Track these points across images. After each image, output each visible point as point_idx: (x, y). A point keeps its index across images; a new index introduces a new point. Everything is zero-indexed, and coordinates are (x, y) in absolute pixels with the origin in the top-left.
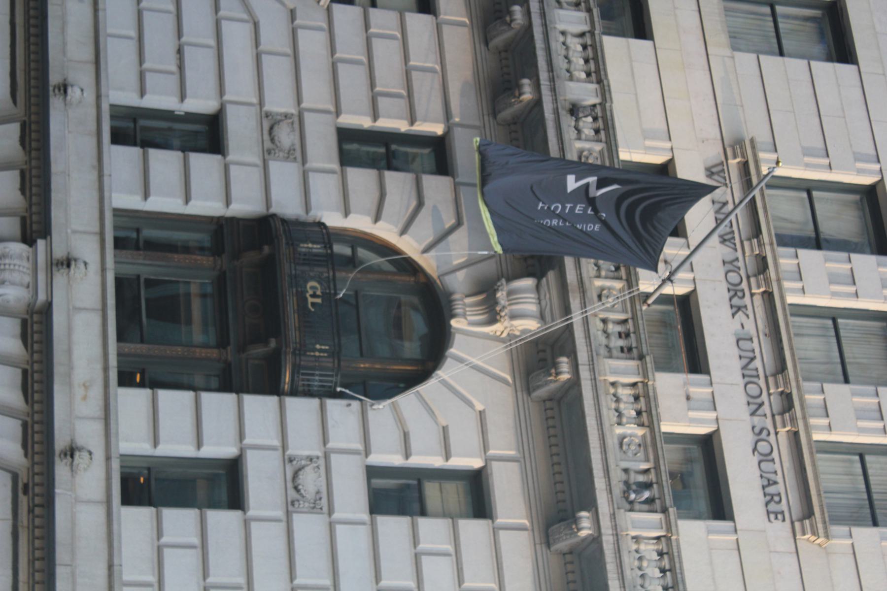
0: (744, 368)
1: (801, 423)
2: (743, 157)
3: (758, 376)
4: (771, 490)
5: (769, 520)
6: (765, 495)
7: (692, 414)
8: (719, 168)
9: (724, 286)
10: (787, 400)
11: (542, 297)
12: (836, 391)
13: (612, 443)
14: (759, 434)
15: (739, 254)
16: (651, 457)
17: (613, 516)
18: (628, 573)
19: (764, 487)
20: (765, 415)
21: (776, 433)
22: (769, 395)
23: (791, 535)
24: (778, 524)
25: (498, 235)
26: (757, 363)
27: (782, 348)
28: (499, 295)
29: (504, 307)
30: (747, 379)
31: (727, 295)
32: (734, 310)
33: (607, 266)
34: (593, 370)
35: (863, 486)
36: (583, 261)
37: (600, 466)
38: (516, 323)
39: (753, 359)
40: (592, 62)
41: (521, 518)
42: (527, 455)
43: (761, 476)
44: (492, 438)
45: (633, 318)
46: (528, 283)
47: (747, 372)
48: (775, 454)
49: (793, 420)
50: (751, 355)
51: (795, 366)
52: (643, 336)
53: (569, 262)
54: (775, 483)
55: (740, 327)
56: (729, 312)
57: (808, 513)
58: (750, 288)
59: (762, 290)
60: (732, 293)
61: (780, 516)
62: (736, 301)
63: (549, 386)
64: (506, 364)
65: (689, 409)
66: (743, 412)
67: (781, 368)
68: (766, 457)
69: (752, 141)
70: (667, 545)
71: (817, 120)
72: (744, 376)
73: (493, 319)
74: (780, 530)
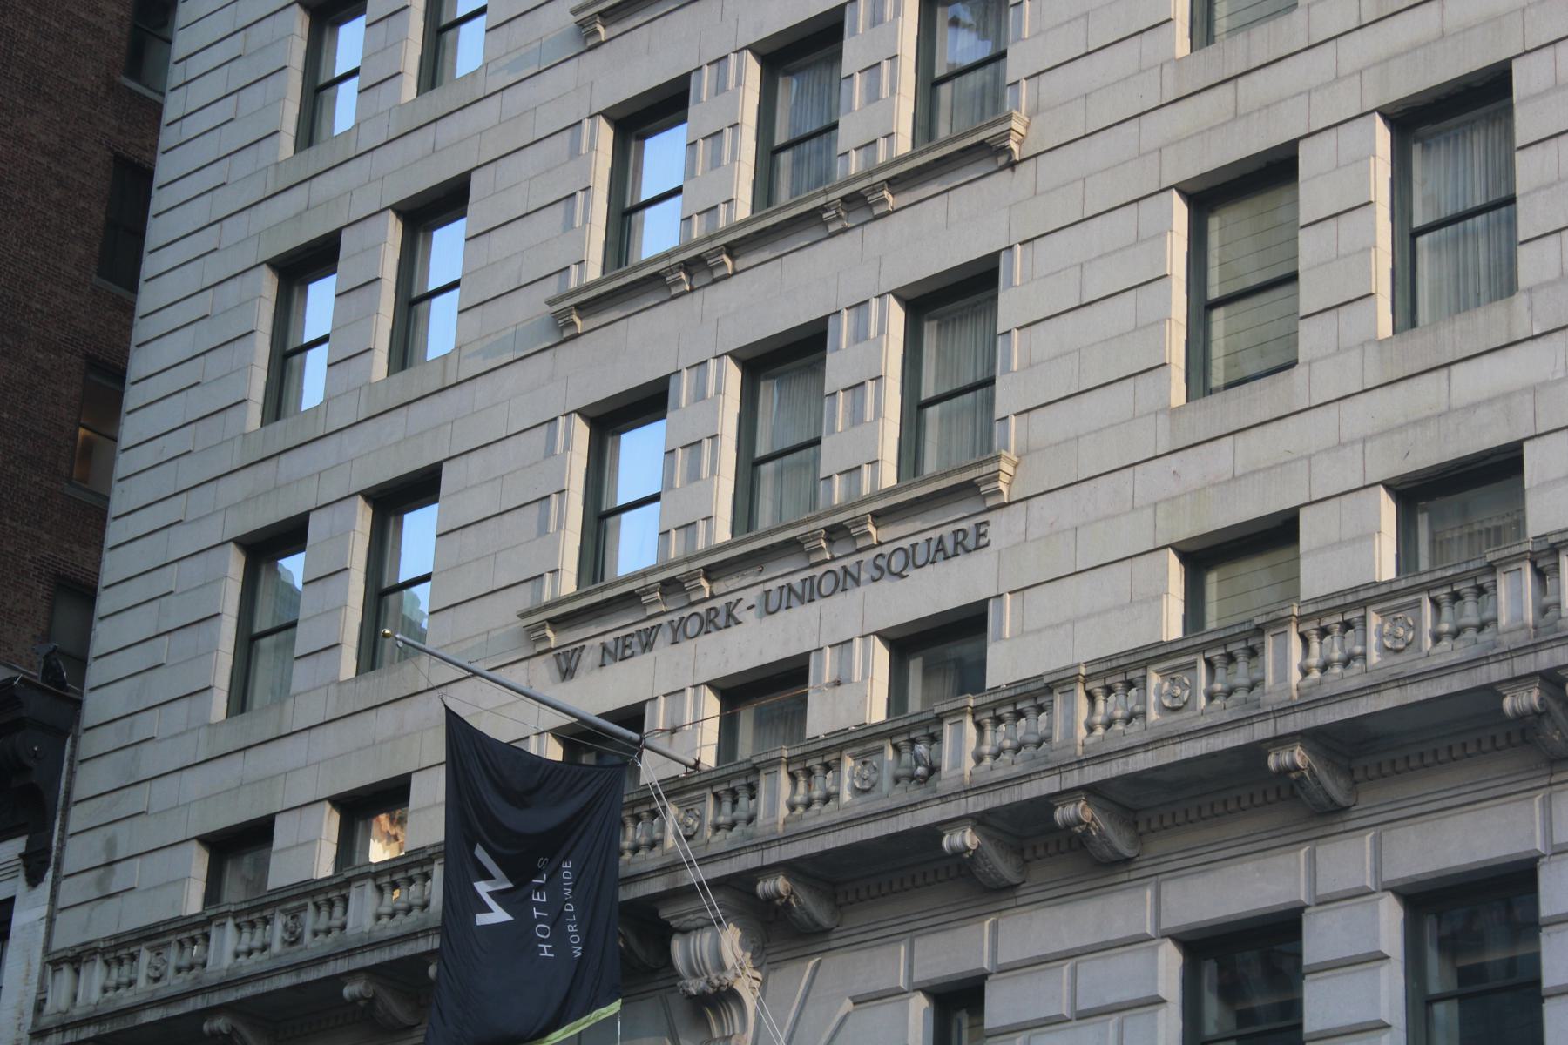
0: (802, 600)
1: (861, 511)
2: (543, 627)
3: (812, 578)
4: (949, 545)
5: (987, 545)
6: (956, 555)
7: (857, 677)
8: (562, 658)
9: (703, 639)
10: (836, 533)
11: (693, 924)
12: (831, 458)
13: (862, 806)
14: (882, 571)
15: (664, 620)
16: (877, 744)
17: (944, 799)
18: (1017, 770)
19: (946, 558)
20: (859, 563)
21: (880, 544)
22: (833, 559)
23: (1005, 510)
24: (992, 532)
25: (599, 1007)
26: (795, 580)
27: (772, 546)
28: (693, 991)
29: (708, 982)
30: (816, 596)
31: (714, 635)
32: (731, 622)
33: (633, 834)
34: (768, 844)
35: (968, 398)
36: (623, 873)
37: (884, 823)
38: (729, 959)
39: (790, 588)
40: (395, 877)
41: (982, 930)
42: (906, 927)
43: (933, 562)
44: (883, 984)
45: (712, 786)
46: (677, 946)
47: (807, 597)
48: (906, 544)
49: (859, 521)
50: (785, 591)
51: (791, 526)
52: (731, 770)
53: (627, 894)
54: (941, 540)
55: (752, 611)
56: (734, 629)
57: (969, 489)
58: (704, 600)
59: (704, 583)
60: (711, 627)
61: (982, 530)
62: (721, 621)
63: (809, 904)
64: (789, 970)
65: (850, 681)
66: (855, 595)
67: (793, 546)
68: (909, 557)
69: (523, 616)
70: (984, 711)
71: (506, 516)
72: (811, 600)
73: (731, 995)
74: (1001, 528)
